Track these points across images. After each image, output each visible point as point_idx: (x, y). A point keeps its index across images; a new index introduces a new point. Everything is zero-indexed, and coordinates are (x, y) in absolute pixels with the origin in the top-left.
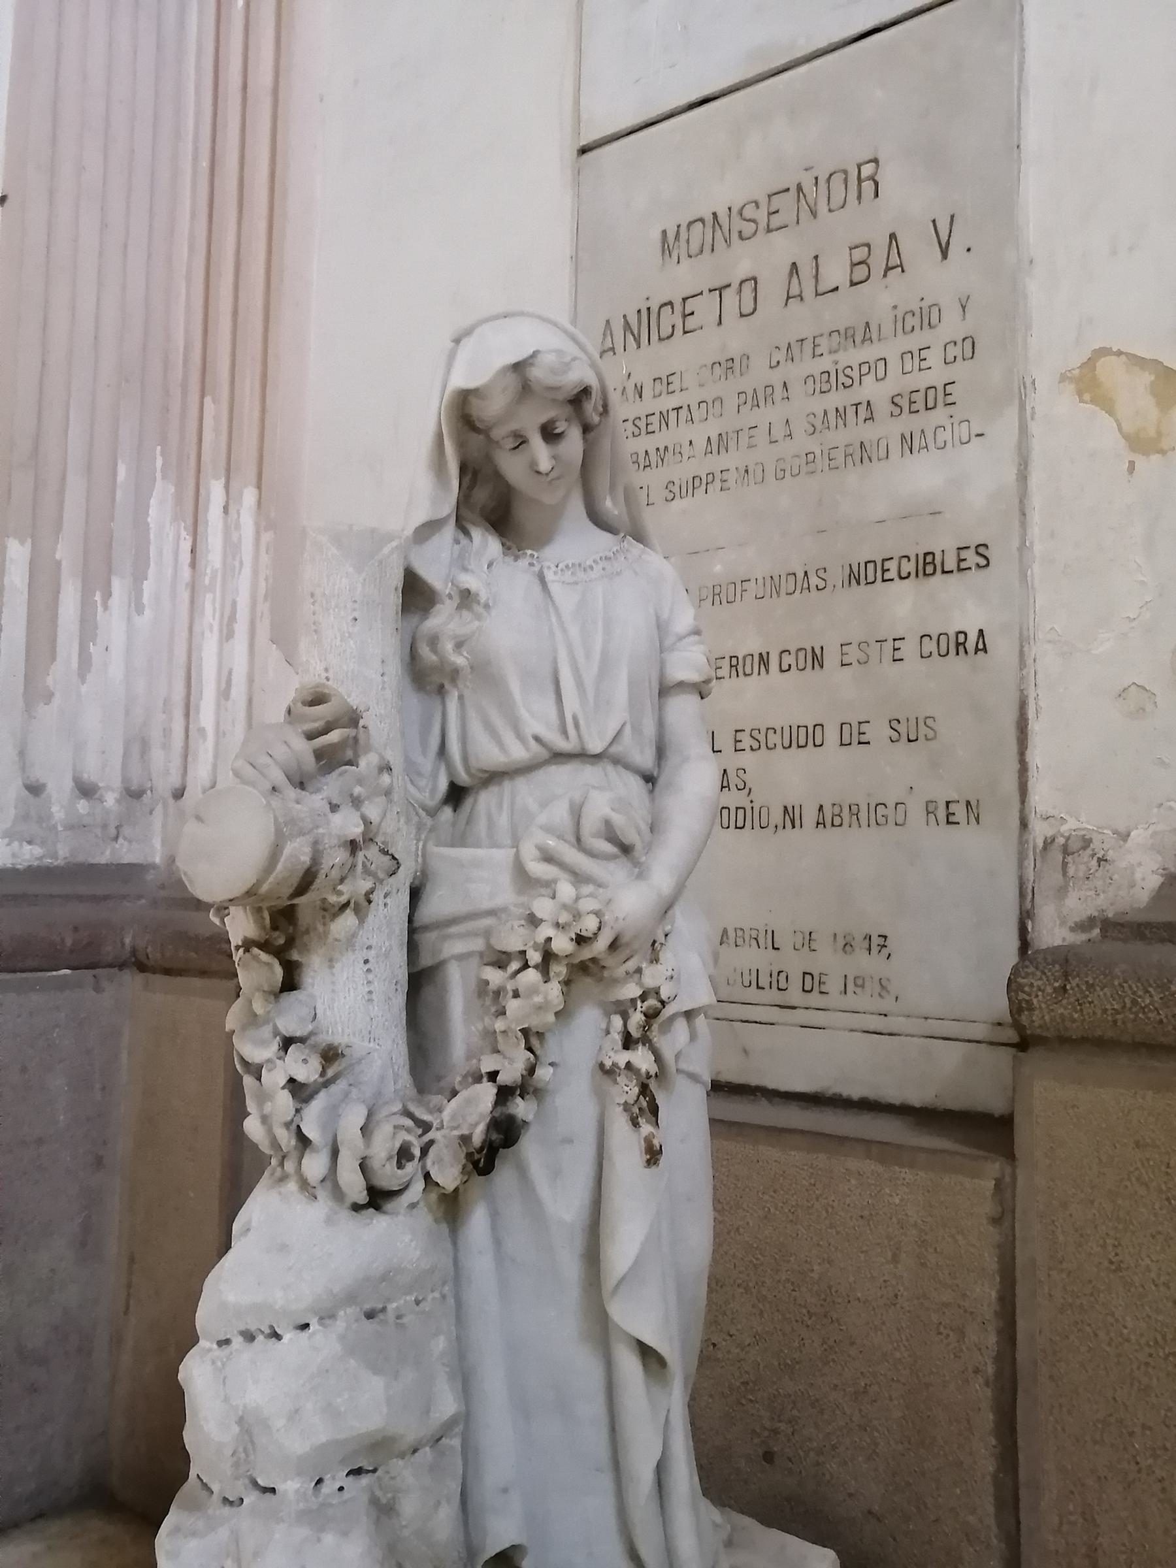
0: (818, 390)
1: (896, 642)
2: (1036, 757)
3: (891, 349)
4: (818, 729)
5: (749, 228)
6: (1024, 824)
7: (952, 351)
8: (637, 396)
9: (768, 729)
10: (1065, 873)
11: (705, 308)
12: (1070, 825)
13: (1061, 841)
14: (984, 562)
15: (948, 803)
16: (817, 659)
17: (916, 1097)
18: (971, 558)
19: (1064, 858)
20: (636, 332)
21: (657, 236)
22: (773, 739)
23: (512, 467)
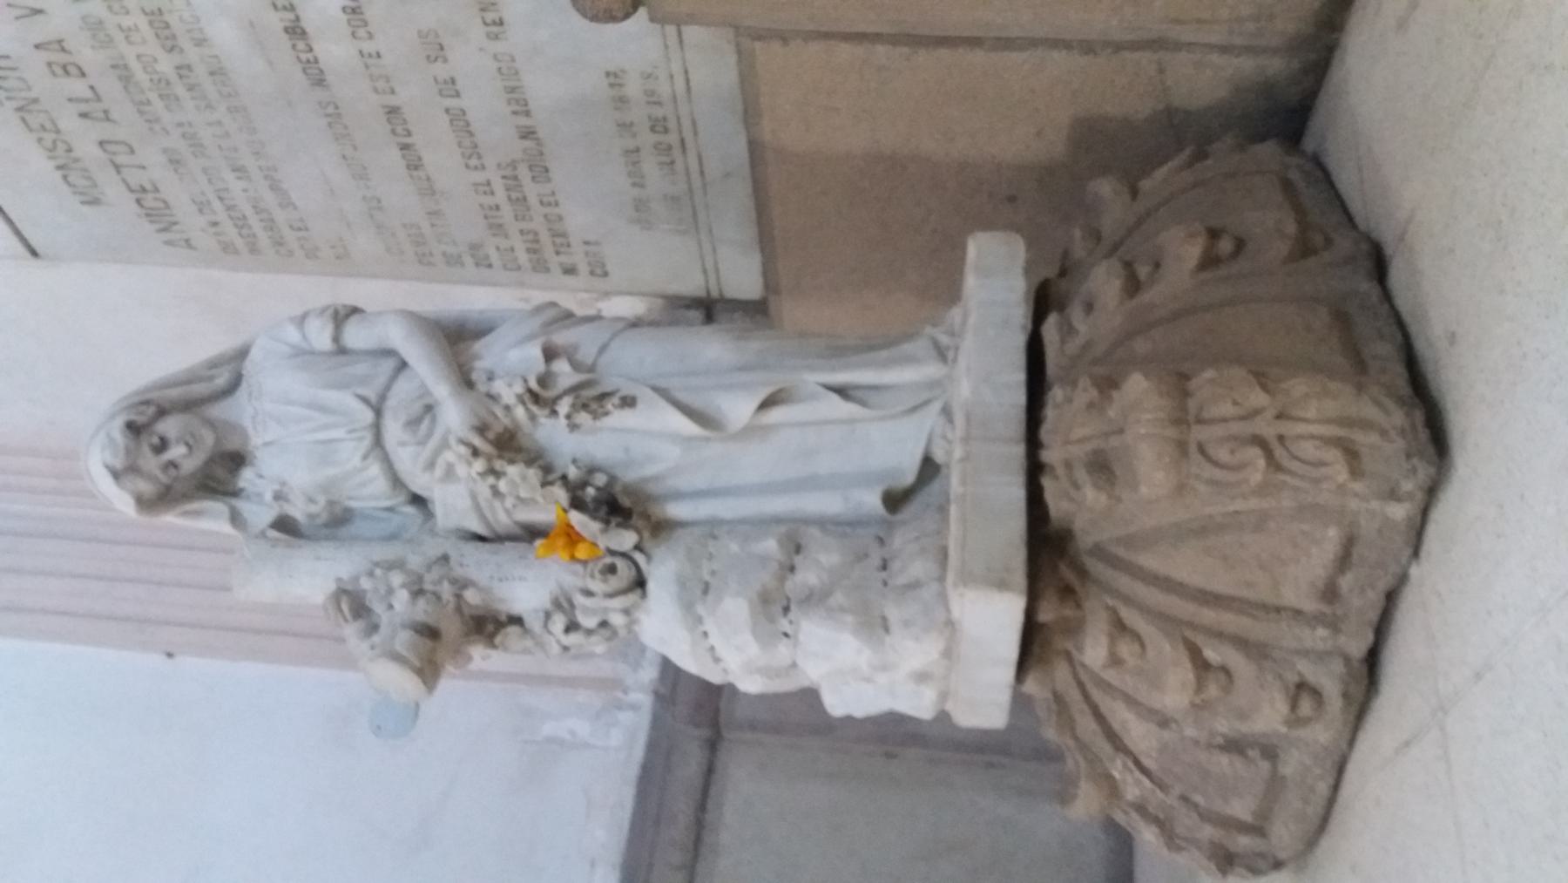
5: (61, 147)
11: (135, 177)
23: (190, 464)
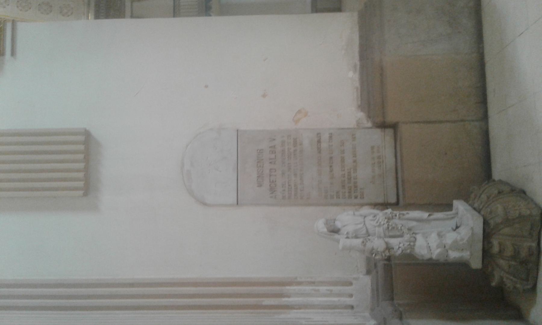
17: (393, 142)
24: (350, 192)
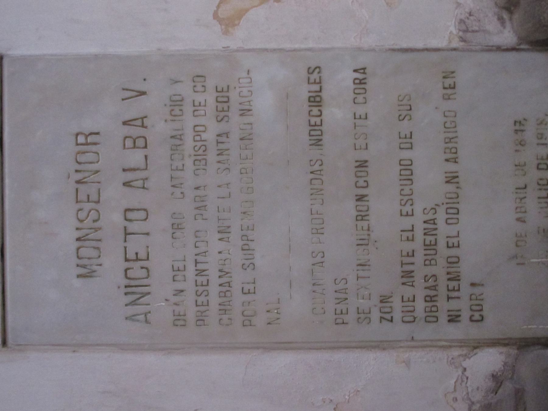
0: (204, 167)
1: (356, 117)
2: (420, 45)
3: (189, 121)
4: (402, 162)
5: (93, 214)
6: (455, 49)
7: (199, 88)
8: (182, 293)
9: (401, 195)
10: (477, 31)
12: (452, 29)
13: (461, 34)
14: (318, 70)
15: (444, 88)
16: (362, 164)
18: (315, 76)
19: (470, 32)
20: (138, 296)
21: (81, 280)
22: (407, 191)
24: (430, 299)
